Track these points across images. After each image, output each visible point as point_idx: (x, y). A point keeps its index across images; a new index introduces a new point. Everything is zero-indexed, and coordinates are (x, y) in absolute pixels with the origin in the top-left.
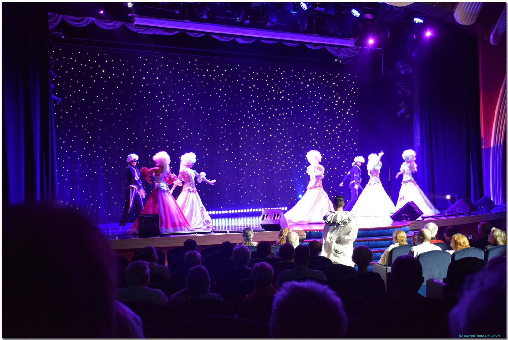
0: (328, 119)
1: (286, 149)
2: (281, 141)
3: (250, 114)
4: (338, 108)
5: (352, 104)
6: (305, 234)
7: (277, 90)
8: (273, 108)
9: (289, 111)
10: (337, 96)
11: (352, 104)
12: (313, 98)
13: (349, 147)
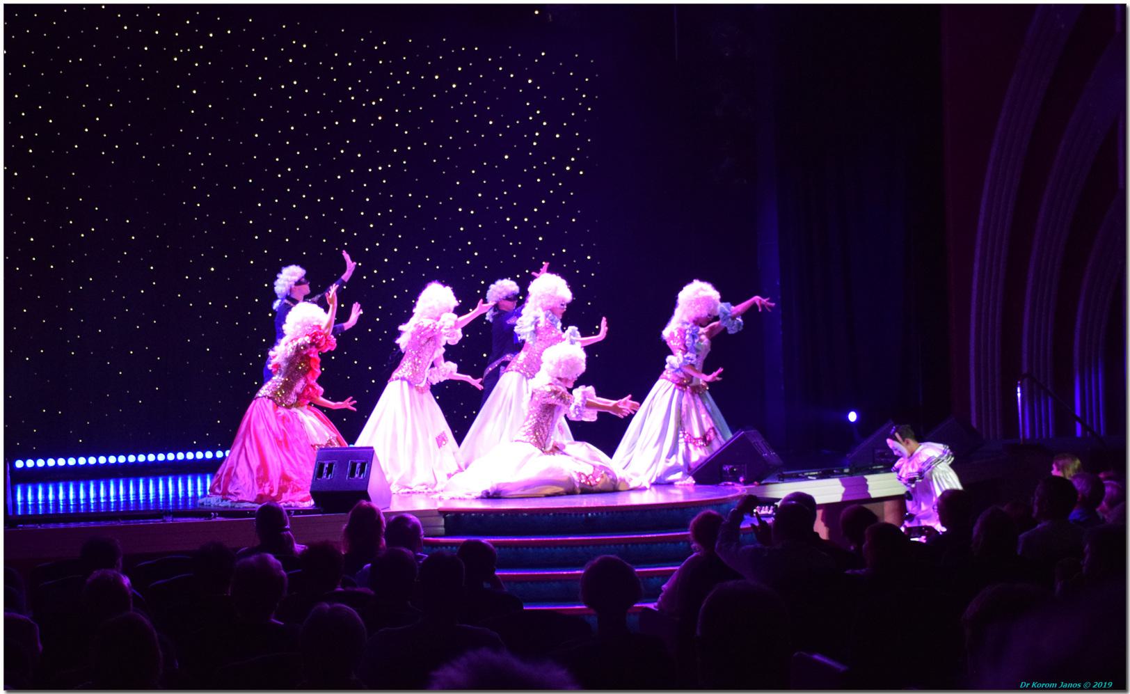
1: (386, 271)
2: (372, 247)
3: (281, 167)
6: (442, 522)
8: (351, 151)
9: (396, 160)
10: (538, 119)
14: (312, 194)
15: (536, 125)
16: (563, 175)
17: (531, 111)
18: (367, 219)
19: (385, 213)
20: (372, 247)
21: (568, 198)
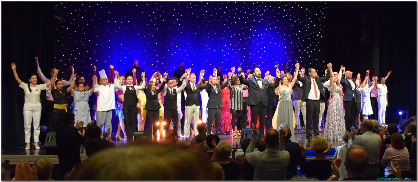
0: (301, 40)
2: (259, 58)
4: (310, 31)
9: (267, 32)
13: (318, 65)
14: (241, 42)
16: (316, 37)
18: (258, 50)
19: (263, 48)
20: (259, 58)
21: (318, 44)
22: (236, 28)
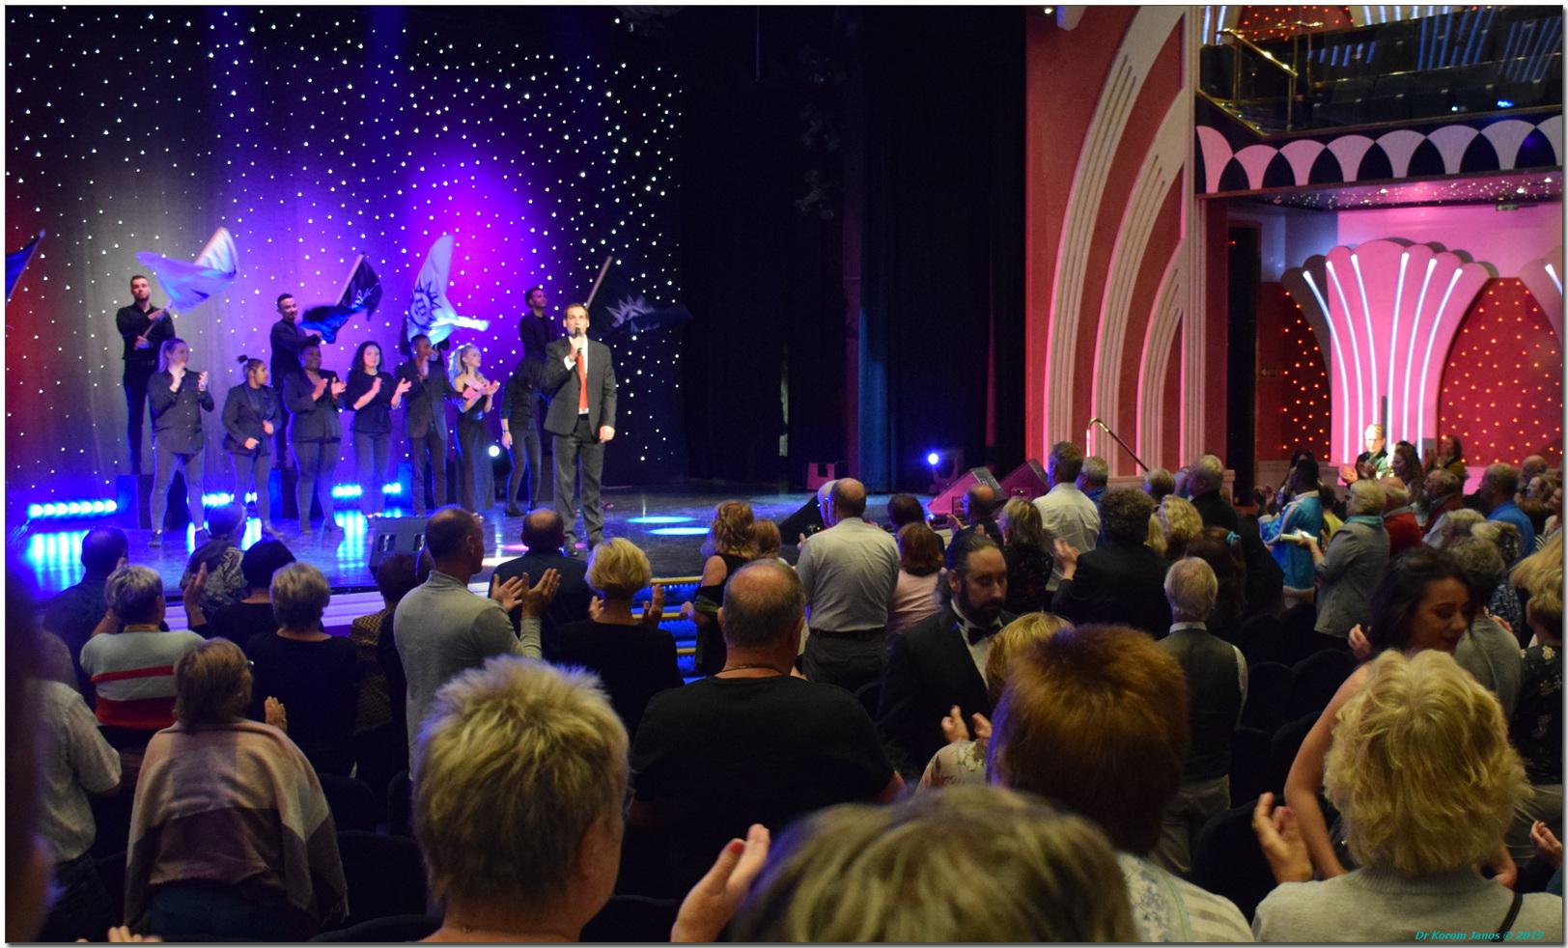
0: (587, 206)
4: (621, 171)
5: (663, 160)
7: (425, 105)
8: (413, 164)
10: (617, 135)
11: (663, 160)
12: (541, 135)
14: (370, 211)
15: (615, 141)
17: (610, 126)
22: (348, 159)
